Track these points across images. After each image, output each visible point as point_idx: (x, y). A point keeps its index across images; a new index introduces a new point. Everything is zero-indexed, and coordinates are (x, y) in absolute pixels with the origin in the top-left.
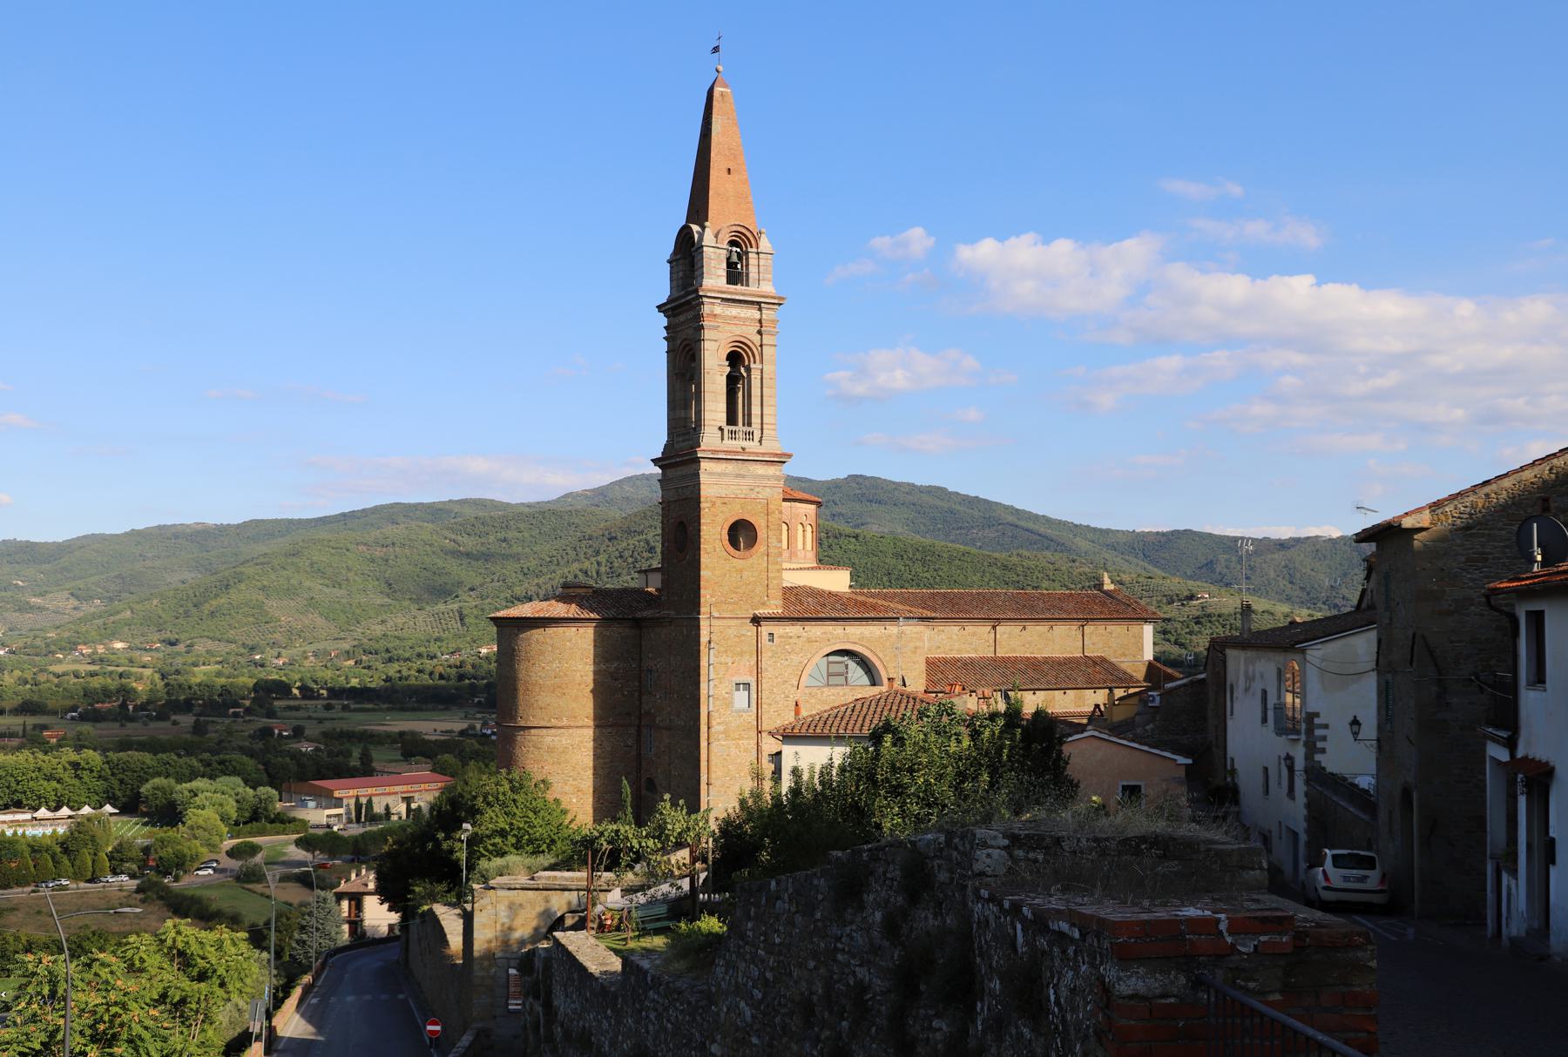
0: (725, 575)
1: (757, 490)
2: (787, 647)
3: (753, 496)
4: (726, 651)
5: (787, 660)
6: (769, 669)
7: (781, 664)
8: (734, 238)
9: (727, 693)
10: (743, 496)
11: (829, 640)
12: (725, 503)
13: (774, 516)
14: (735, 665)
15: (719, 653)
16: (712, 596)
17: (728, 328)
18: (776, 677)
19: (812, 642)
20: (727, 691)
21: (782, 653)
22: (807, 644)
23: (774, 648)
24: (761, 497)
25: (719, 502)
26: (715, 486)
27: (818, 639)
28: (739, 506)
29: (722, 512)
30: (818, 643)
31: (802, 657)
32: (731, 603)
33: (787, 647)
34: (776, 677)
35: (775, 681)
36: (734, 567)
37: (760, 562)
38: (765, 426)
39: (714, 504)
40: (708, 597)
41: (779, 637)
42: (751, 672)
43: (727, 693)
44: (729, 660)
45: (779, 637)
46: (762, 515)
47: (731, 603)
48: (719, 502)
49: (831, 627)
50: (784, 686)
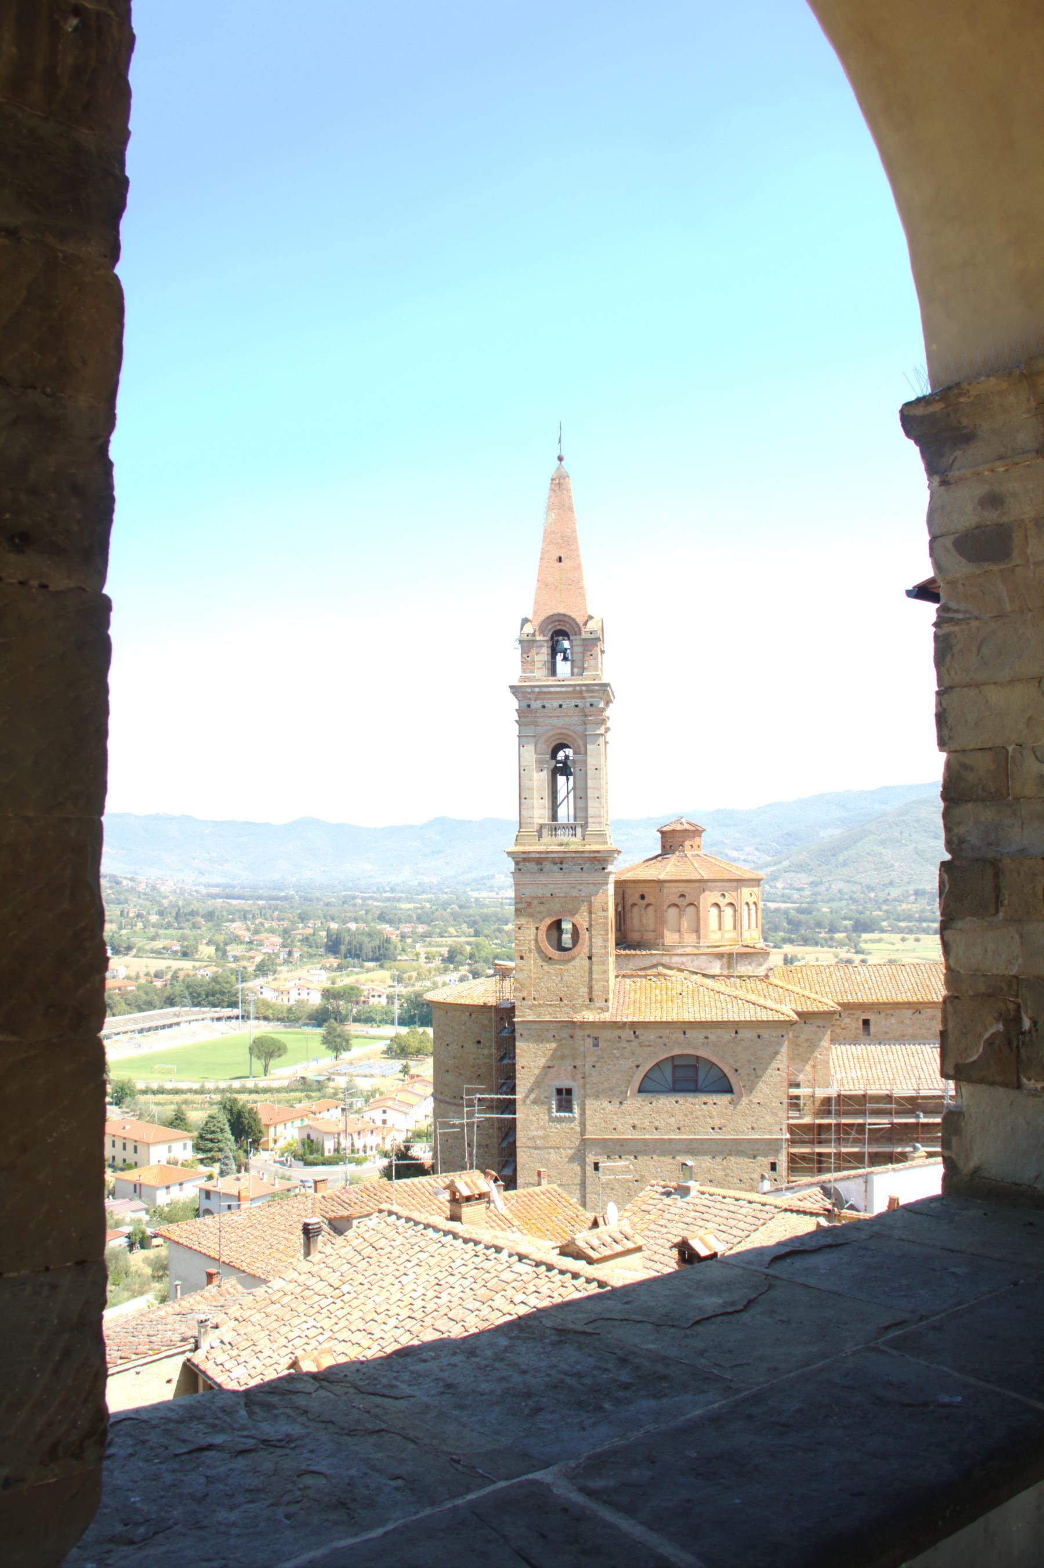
2: (615, 1051)
3: (574, 894)
6: (594, 1074)
7: (608, 1069)
9: (546, 1097)
10: (562, 895)
11: (665, 1045)
12: (542, 903)
17: (548, 721)
18: (602, 1083)
20: (546, 1095)
21: (609, 1058)
23: (599, 1052)
25: (535, 902)
26: (531, 886)
27: (652, 1043)
28: (559, 905)
34: (602, 1083)
39: (529, 904)
41: (606, 1040)
43: (546, 1097)
45: (606, 1040)
48: (535, 902)
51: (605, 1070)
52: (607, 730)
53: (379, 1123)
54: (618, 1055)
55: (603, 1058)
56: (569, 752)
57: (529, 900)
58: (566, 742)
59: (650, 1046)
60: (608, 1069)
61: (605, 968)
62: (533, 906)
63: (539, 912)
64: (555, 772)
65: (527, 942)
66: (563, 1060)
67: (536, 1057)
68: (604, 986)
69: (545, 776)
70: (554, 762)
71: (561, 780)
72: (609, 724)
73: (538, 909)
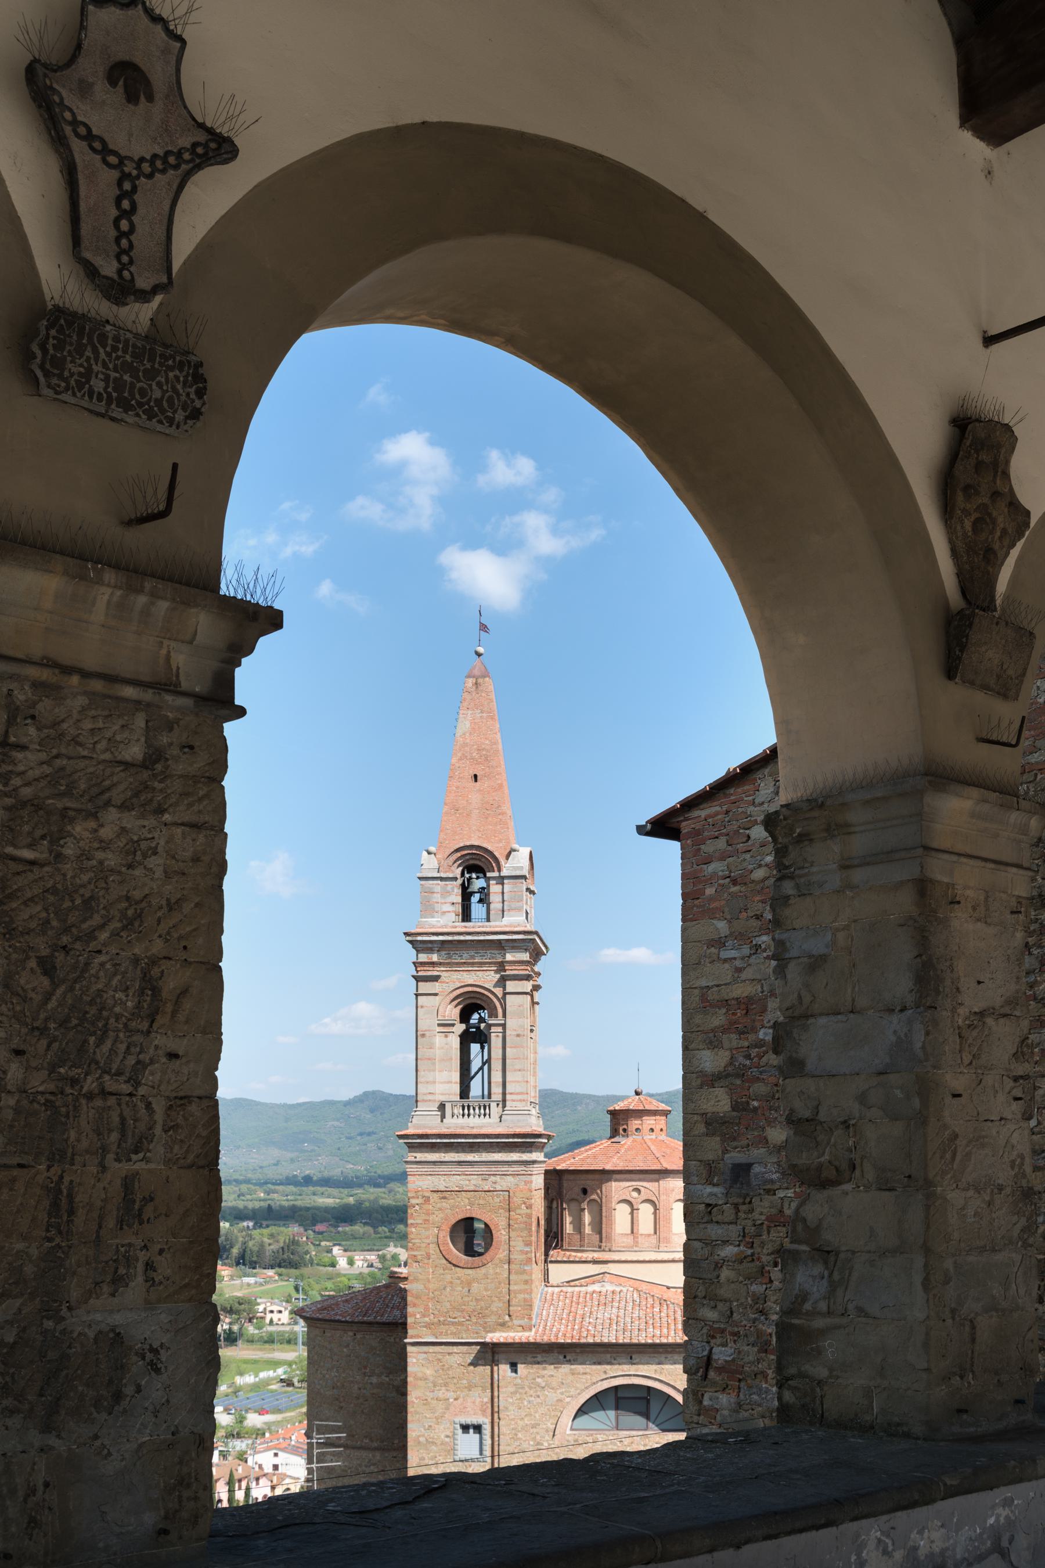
0: (444, 1289)
1: (493, 1178)
2: (539, 1380)
3: (486, 1188)
4: (446, 1385)
5: (538, 1397)
6: (511, 1408)
7: (529, 1402)
8: (471, 862)
10: (472, 1188)
12: (445, 1198)
13: (518, 1211)
14: (460, 1401)
15: (435, 1386)
16: (424, 1316)
18: (522, 1419)
19: (579, 1374)
21: (530, 1388)
22: (571, 1377)
23: (519, 1381)
24: (499, 1188)
29: (440, 1209)
30: (589, 1377)
31: (562, 1393)
32: (453, 1324)
33: (539, 1380)
34: (522, 1419)
35: (521, 1423)
36: (459, 1278)
37: (498, 1271)
38: (508, 1097)
39: (427, 1200)
40: (418, 1316)
42: (484, 1411)
44: (451, 1395)
46: (501, 1211)
47: (453, 1324)
49: (608, 1356)
50: (535, 1430)
51: (526, 1403)
52: (536, 988)
53: (268, 1469)
54: (543, 1384)
55: (523, 1388)
56: (485, 1014)
57: (427, 1194)
58: (479, 1002)
59: (585, 1373)
60: (529, 1402)
61: (525, 1277)
62: (432, 1201)
63: (440, 1209)
64: (466, 1039)
65: (423, 1245)
66: (470, 1390)
67: (435, 1386)
68: (525, 1300)
69: (455, 1042)
70: (463, 1027)
71: (475, 1048)
72: (539, 981)
73: (439, 1205)
